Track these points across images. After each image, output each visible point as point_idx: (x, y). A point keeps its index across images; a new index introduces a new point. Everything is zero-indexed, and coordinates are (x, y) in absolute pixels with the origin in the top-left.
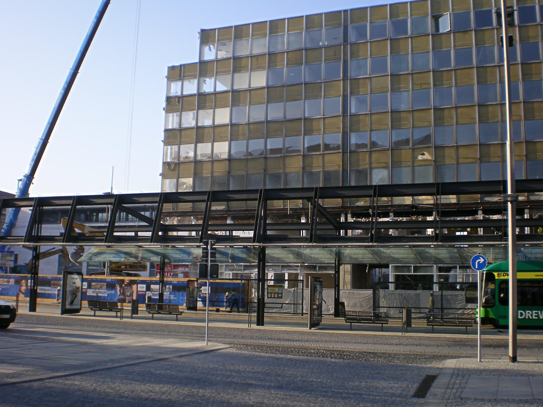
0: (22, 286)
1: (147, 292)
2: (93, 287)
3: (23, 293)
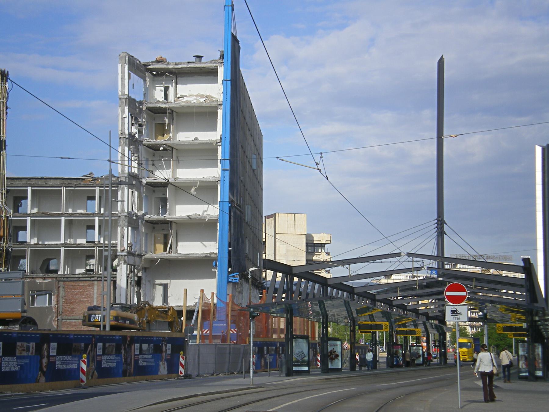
0: (44, 357)
1: (140, 356)
2: (106, 352)
3: (44, 373)
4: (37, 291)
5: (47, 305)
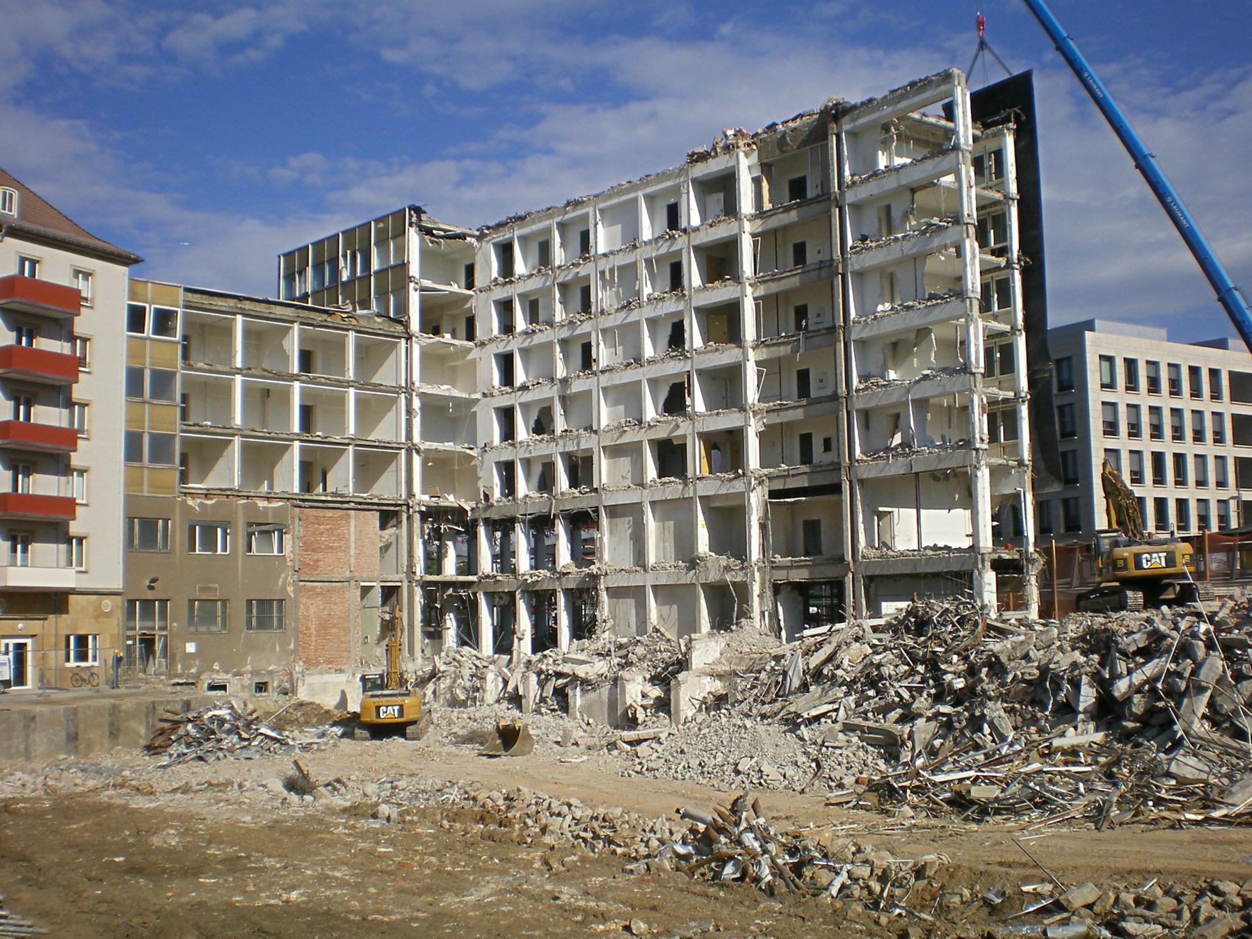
4: (258, 524)
5: (276, 553)
